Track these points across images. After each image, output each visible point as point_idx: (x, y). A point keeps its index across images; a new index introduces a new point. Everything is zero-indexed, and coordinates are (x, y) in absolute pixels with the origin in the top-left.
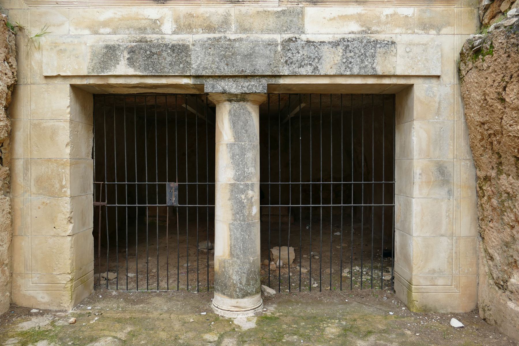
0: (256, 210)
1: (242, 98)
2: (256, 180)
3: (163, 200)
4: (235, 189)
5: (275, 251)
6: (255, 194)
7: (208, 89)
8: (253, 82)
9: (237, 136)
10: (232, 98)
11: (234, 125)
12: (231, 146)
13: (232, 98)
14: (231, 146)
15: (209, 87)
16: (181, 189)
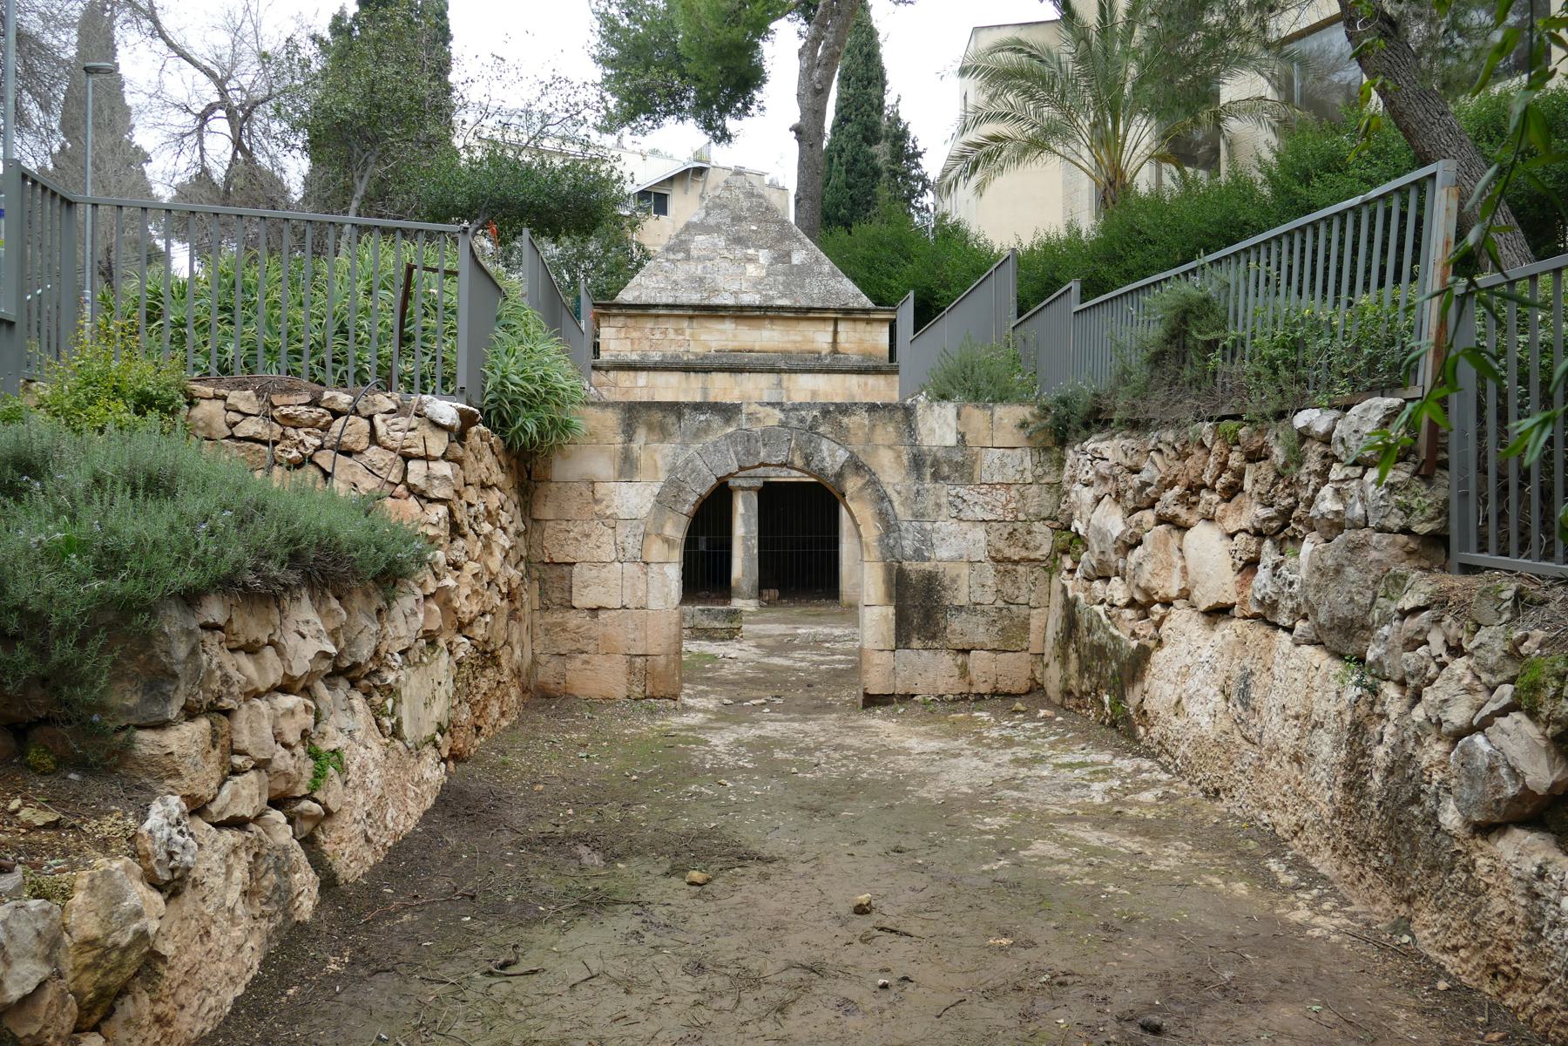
0: (756, 551)
1: (749, 489)
2: (756, 534)
3: (697, 547)
4: (745, 539)
5: (765, 592)
6: (755, 542)
7: (731, 484)
8: (755, 480)
9: (746, 509)
10: (743, 489)
11: (745, 503)
12: (742, 515)
13: (743, 489)
14: (742, 515)
15: (732, 483)
16: (708, 541)
